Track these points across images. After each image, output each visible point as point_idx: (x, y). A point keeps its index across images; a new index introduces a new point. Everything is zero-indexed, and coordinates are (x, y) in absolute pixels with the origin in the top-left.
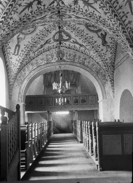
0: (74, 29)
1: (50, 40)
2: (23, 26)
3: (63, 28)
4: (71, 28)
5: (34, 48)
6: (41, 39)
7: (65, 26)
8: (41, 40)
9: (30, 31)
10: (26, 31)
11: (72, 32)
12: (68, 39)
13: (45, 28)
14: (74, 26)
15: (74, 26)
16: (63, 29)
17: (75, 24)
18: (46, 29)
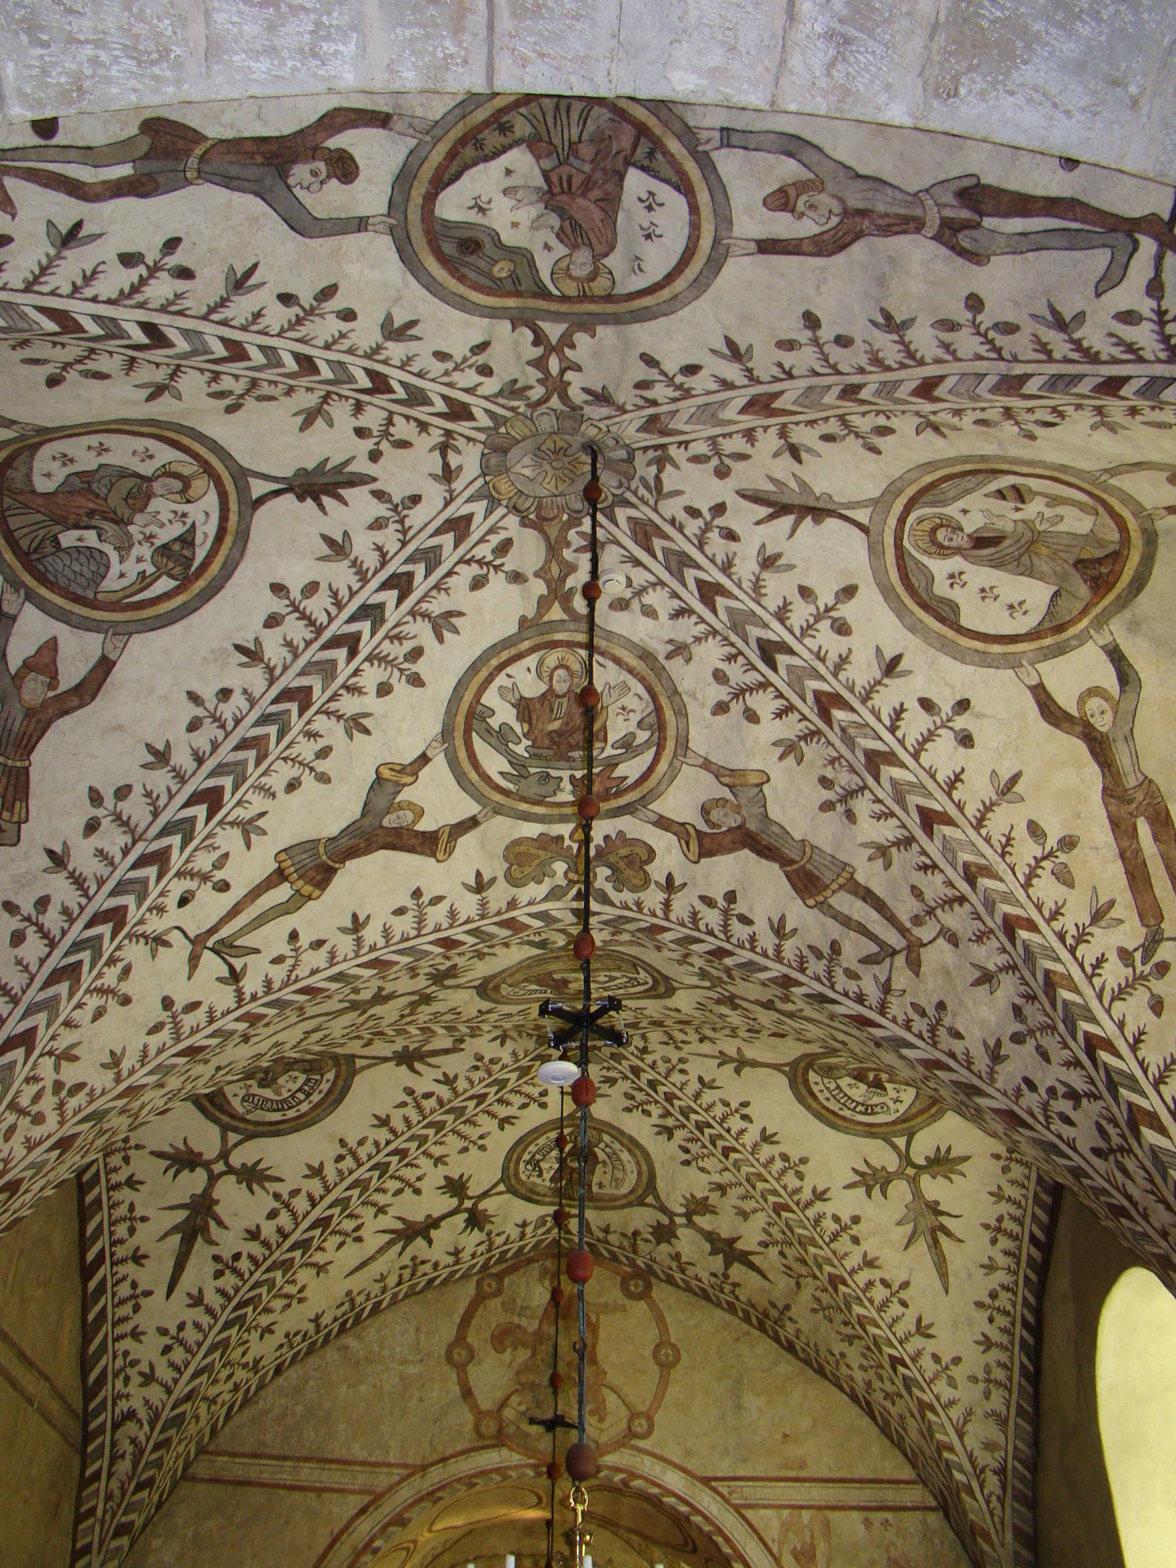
0: (380, 384)
1: (783, 226)
2: (902, 978)
3: (540, 364)
4: (417, 397)
5: (1094, 336)
6: (913, 357)
7: (513, 390)
8: (924, 338)
9: (1000, 494)
10: (1049, 513)
11: (395, 332)
12: (442, 181)
13: (795, 452)
14: (386, 434)
15: (386, 434)
16: (539, 339)
17: (375, 456)
18: (783, 433)
